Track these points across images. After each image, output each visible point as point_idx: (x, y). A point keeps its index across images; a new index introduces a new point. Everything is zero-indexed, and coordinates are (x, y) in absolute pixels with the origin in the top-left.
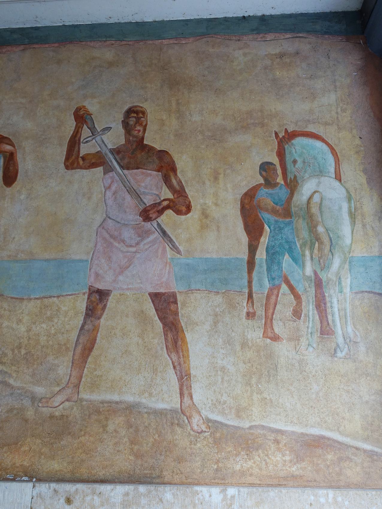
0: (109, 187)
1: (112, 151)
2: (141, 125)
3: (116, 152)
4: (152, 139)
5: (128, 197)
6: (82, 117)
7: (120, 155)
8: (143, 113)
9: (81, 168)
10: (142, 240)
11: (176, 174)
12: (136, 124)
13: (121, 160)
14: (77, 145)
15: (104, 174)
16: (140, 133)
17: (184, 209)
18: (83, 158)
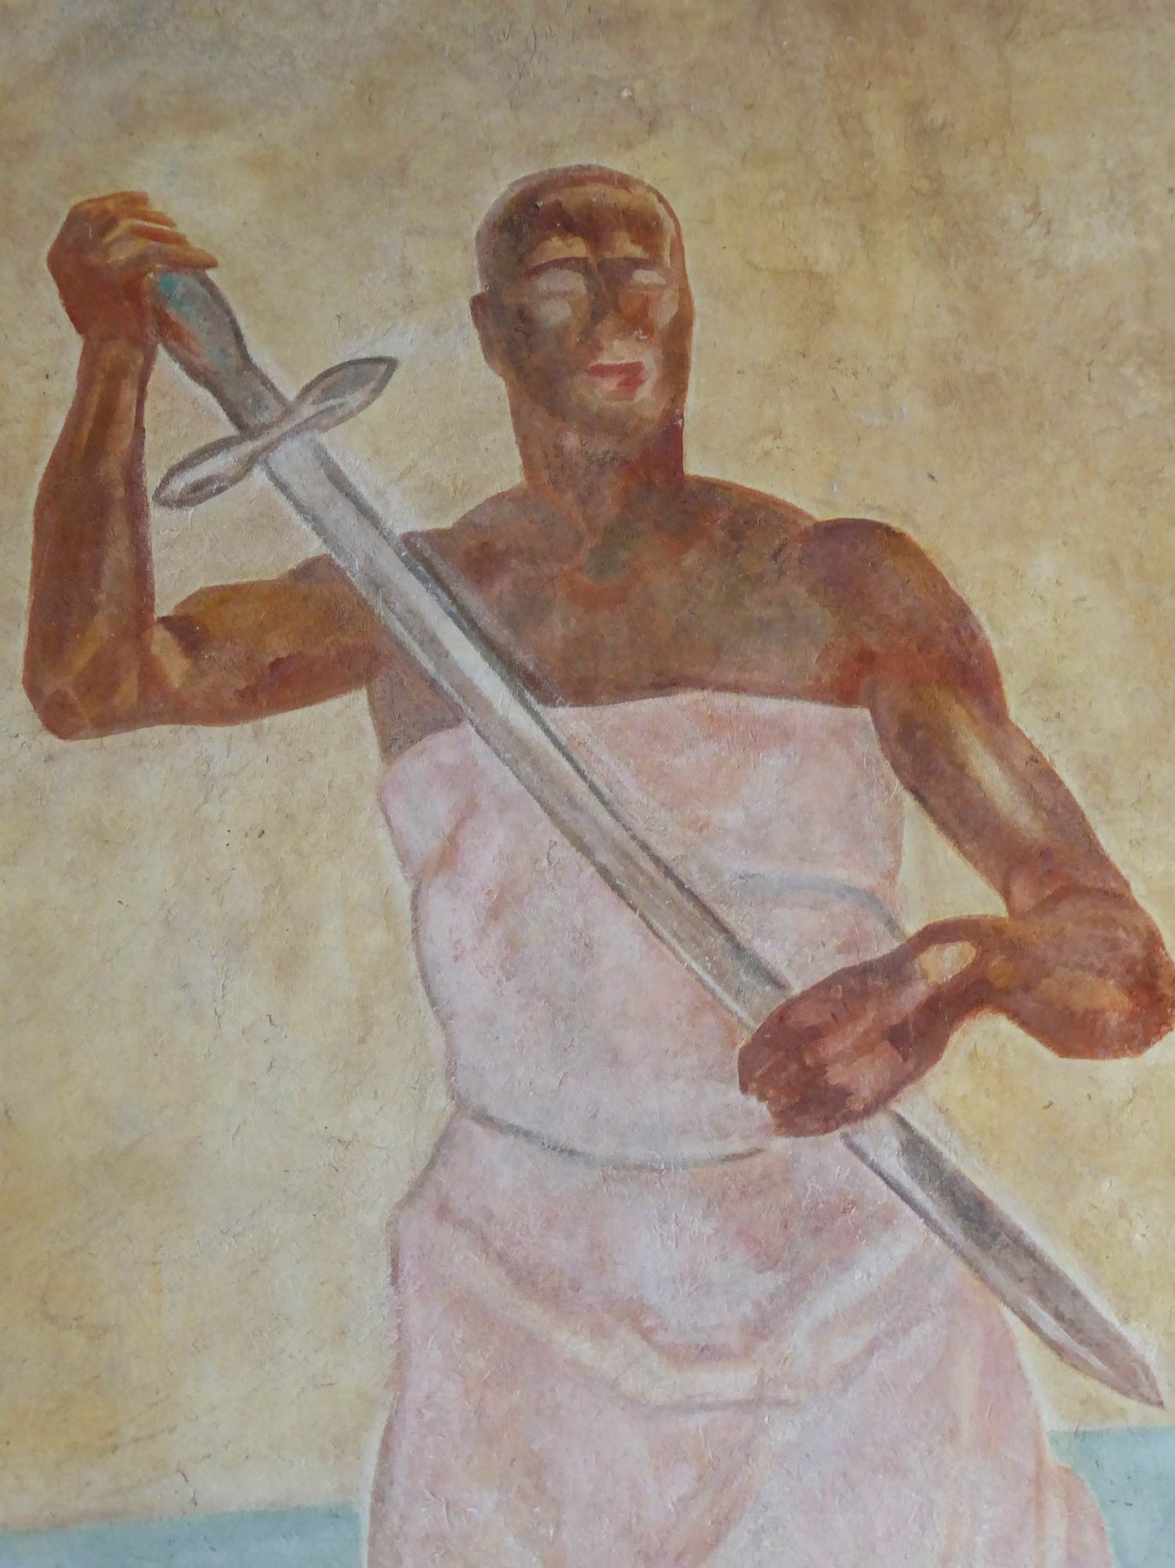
0: (448, 858)
1: (425, 554)
2: (637, 322)
3: (465, 557)
4: (752, 428)
5: (619, 932)
6: (124, 290)
7: (503, 585)
8: (646, 227)
9: (180, 712)
10: (794, 1294)
11: (996, 715)
12: (596, 316)
13: (512, 621)
14: (118, 525)
15: (391, 746)
16: (645, 392)
17: (1110, 999)
18: (189, 630)
